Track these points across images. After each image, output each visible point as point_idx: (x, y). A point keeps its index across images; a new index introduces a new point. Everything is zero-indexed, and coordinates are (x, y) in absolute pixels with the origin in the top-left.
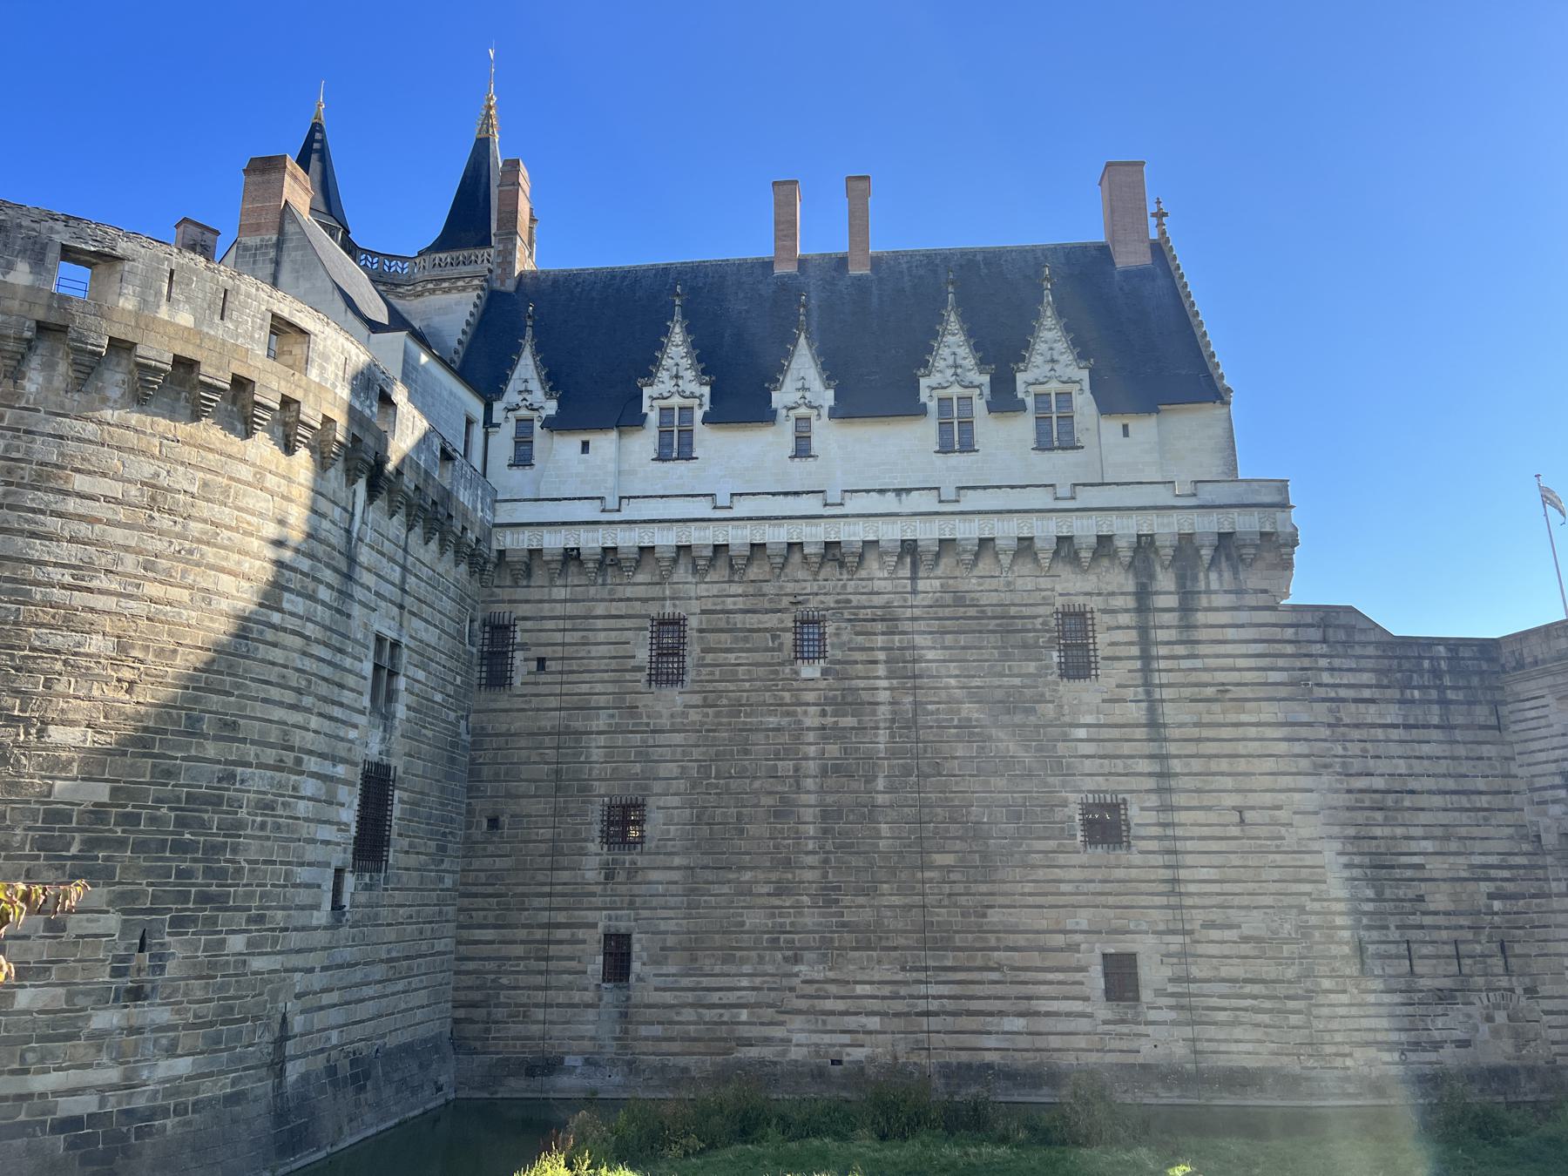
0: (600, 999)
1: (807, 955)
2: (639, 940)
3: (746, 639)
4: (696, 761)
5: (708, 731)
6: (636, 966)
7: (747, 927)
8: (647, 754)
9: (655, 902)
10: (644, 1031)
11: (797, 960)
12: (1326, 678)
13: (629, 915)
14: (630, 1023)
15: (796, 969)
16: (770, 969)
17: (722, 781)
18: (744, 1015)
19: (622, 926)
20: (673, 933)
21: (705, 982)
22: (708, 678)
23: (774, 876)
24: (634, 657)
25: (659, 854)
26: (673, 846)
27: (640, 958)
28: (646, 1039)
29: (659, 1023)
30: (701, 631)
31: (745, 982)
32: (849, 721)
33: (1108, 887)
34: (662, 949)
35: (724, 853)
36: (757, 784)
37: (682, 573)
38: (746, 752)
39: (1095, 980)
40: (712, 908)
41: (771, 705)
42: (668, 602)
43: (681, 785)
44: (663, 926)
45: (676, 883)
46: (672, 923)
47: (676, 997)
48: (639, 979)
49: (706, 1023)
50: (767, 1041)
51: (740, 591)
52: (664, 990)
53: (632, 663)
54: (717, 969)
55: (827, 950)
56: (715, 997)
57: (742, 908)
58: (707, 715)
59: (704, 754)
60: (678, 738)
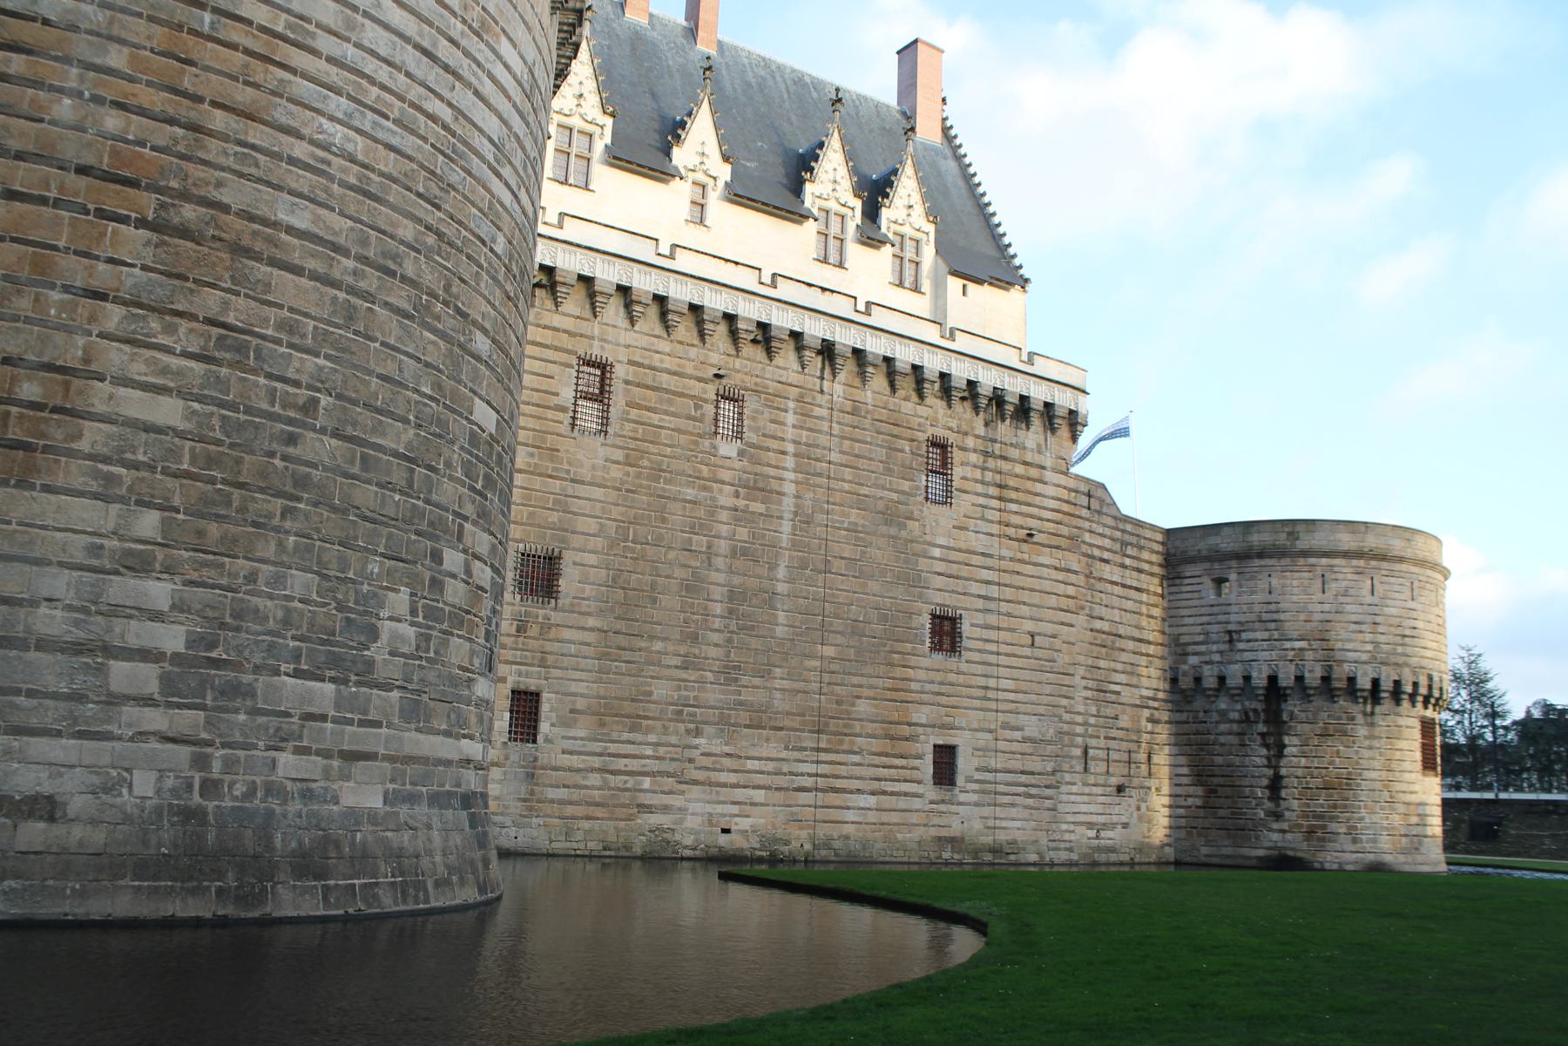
0: (507, 758)
1: (709, 730)
2: (549, 700)
3: (670, 402)
4: (615, 520)
5: (628, 491)
6: (544, 727)
7: (654, 697)
8: (566, 503)
9: (566, 661)
10: (551, 793)
11: (698, 733)
12: (1087, 537)
13: (539, 673)
14: (537, 784)
15: (697, 741)
16: (673, 739)
17: (639, 546)
18: (647, 783)
19: (532, 684)
20: (582, 696)
21: (613, 748)
22: (631, 434)
23: (683, 650)
24: (557, 394)
25: (573, 612)
26: (589, 606)
27: (548, 718)
28: (552, 801)
29: (565, 786)
30: (627, 382)
31: (649, 752)
32: (758, 507)
33: (944, 689)
34: (572, 711)
35: (637, 621)
36: (672, 555)
37: (613, 311)
38: (664, 520)
39: (927, 767)
40: (623, 674)
41: (690, 476)
42: (596, 343)
43: (599, 543)
44: (574, 688)
45: (588, 644)
46: (583, 687)
47: (584, 761)
48: (547, 740)
49: (610, 789)
50: (666, 809)
51: (667, 350)
52: (571, 753)
53: (555, 400)
54: (625, 736)
55: (725, 724)
56: (621, 764)
57: (652, 677)
58: (628, 474)
59: (622, 514)
60: (598, 493)
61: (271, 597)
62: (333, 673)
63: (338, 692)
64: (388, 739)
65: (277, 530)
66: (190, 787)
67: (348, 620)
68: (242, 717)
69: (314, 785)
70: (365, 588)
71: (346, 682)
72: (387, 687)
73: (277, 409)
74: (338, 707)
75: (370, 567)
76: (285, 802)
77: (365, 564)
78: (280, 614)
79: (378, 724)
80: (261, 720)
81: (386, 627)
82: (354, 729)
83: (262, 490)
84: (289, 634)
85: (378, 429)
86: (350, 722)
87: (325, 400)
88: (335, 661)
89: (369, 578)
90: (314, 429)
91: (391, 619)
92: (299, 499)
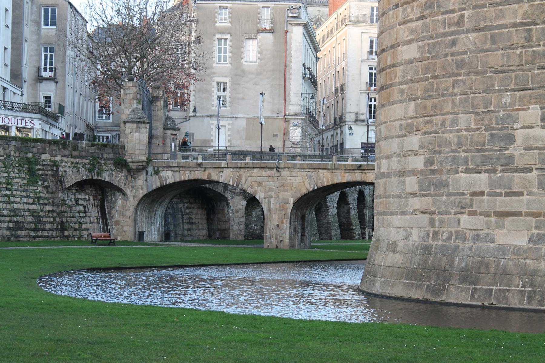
61: (451, 132)
62: (486, 168)
63: (490, 177)
64: (529, 203)
65: (451, 95)
66: (428, 235)
67: (492, 135)
68: (444, 198)
69: (481, 232)
70: (501, 113)
71: (494, 171)
72: (527, 170)
73: (447, 30)
74: (491, 186)
75: (504, 100)
76: (464, 242)
77: (501, 99)
78: (456, 140)
79: (521, 194)
80: (452, 198)
81: (520, 135)
82: (503, 198)
83: (444, 76)
84: (462, 149)
85: (501, 15)
86: (500, 194)
87: (467, 13)
88: (487, 160)
89: (504, 107)
90: (463, 33)
91: (524, 127)
92: (460, 75)
